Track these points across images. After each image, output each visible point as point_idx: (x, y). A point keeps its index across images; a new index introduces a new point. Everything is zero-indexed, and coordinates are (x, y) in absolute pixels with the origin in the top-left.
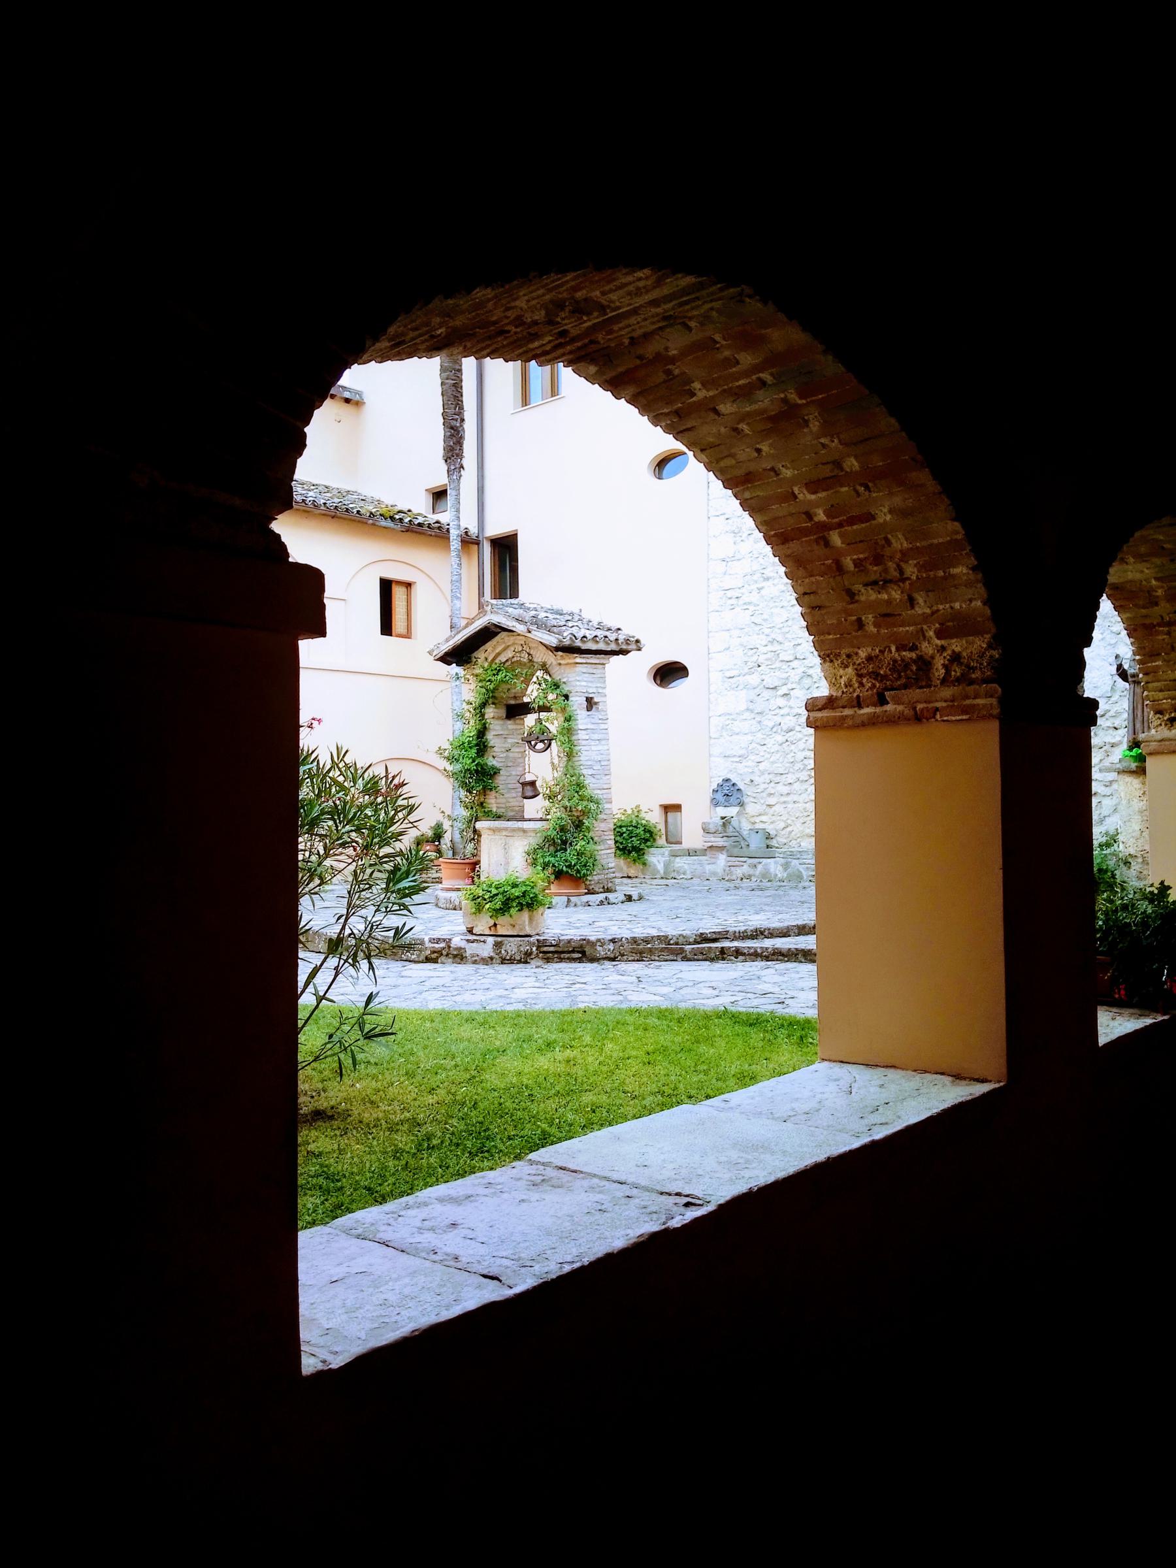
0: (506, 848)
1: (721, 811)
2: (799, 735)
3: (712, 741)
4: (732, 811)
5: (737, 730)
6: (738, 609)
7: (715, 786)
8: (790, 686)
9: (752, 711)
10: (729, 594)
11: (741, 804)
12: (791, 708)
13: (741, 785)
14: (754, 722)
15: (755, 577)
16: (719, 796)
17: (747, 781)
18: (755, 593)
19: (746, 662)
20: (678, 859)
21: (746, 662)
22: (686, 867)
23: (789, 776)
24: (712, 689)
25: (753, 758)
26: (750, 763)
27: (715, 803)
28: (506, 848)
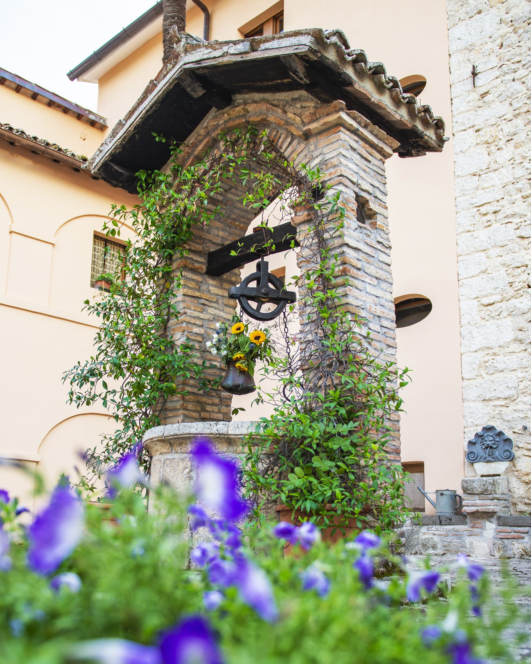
1: (481, 468)
3: (466, 382)
4: (501, 467)
5: (501, 366)
6: (495, 226)
7: (472, 437)
9: (521, 341)
10: (483, 210)
11: (511, 458)
13: (508, 434)
14: (525, 354)
15: (519, 185)
16: (478, 449)
17: (519, 428)
18: (520, 202)
19: (511, 284)
20: (424, 529)
21: (511, 284)
22: (436, 539)
24: (464, 321)
25: (522, 398)
26: (520, 407)
27: (472, 458)
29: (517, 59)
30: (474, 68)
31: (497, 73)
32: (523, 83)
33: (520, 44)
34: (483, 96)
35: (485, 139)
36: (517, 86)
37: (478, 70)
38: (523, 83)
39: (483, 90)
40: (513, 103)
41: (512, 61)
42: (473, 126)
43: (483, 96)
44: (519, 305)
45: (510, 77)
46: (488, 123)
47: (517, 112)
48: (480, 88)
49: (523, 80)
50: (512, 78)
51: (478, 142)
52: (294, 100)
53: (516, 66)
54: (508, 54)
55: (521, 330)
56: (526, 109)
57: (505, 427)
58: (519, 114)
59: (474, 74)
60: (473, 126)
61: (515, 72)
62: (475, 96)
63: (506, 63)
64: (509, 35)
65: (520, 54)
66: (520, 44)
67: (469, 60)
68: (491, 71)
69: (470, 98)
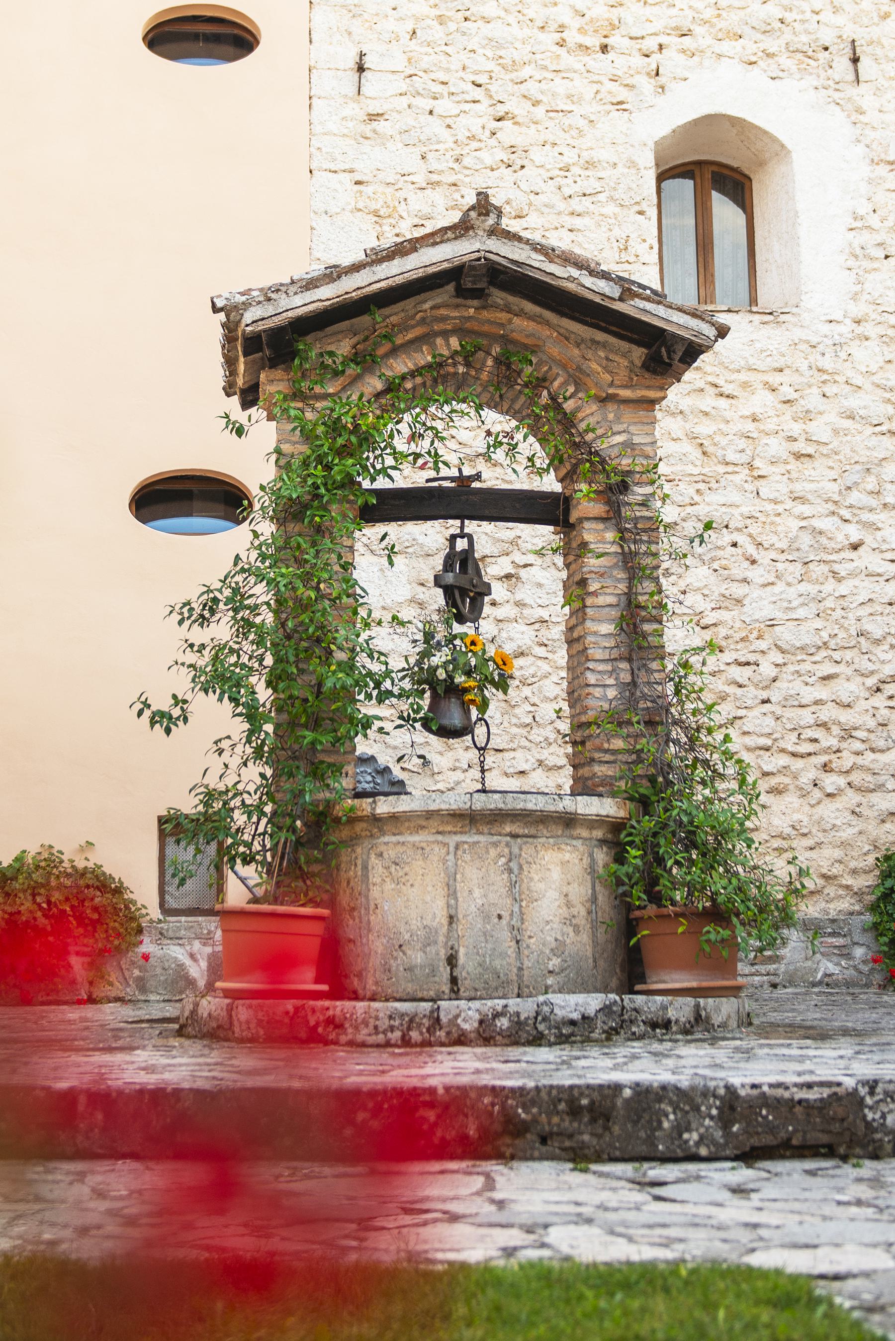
0: (514, 873)
2: (545, 667)
8: (521, 559)
12: (519, 604)
23: (519, 754)
28: (514, 873)
29: (442, 77)
30: (362, 55)
31: (403, 86)
32: (449, 126)
33: (448, 49)
34: (373, 117)
35: (373, 206)
36: (435, 127)
37: (368, 63)
38: (449, 126)
39: (375, 107)
40: (430, 156)
41: (433, 76)
42: (351, 171)
43: (373, 117)
44: (421, 539)
45: (426, 104)
46: (381, 176)
47: (435, 177)
48: (369, 101)
49: (449, 121)
50: (428, 109)
51: (360, 205)
52: (604, 345)
53: (438, 88)
54: (426, 58)
55: (423, 585)
56: (452, 179)
57: (388, 758)
58: (438, 183)
59: (361, 69)
60: (351, 171)
61: (435, 98)
62: (357, 111)
63: (421, 74)
64: (429, 22)
65: (448, 70)
66: (448, 49)
67: (350, 33)
68: (390, 76)
69: (347, 111)
